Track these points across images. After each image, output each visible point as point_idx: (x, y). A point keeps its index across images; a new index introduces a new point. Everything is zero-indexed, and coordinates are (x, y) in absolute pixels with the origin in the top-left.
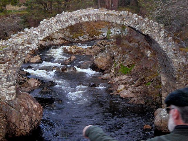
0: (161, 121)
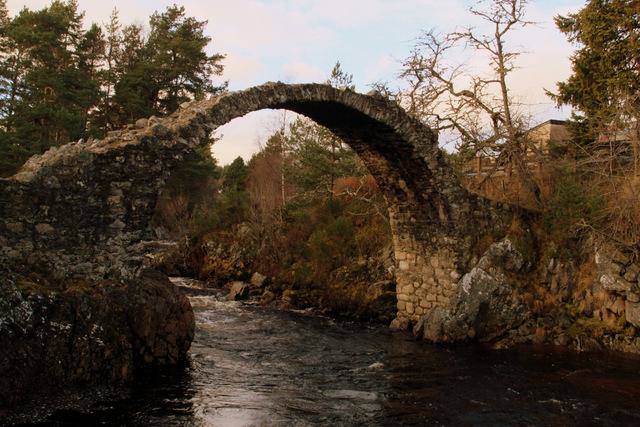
0: (442, 332)
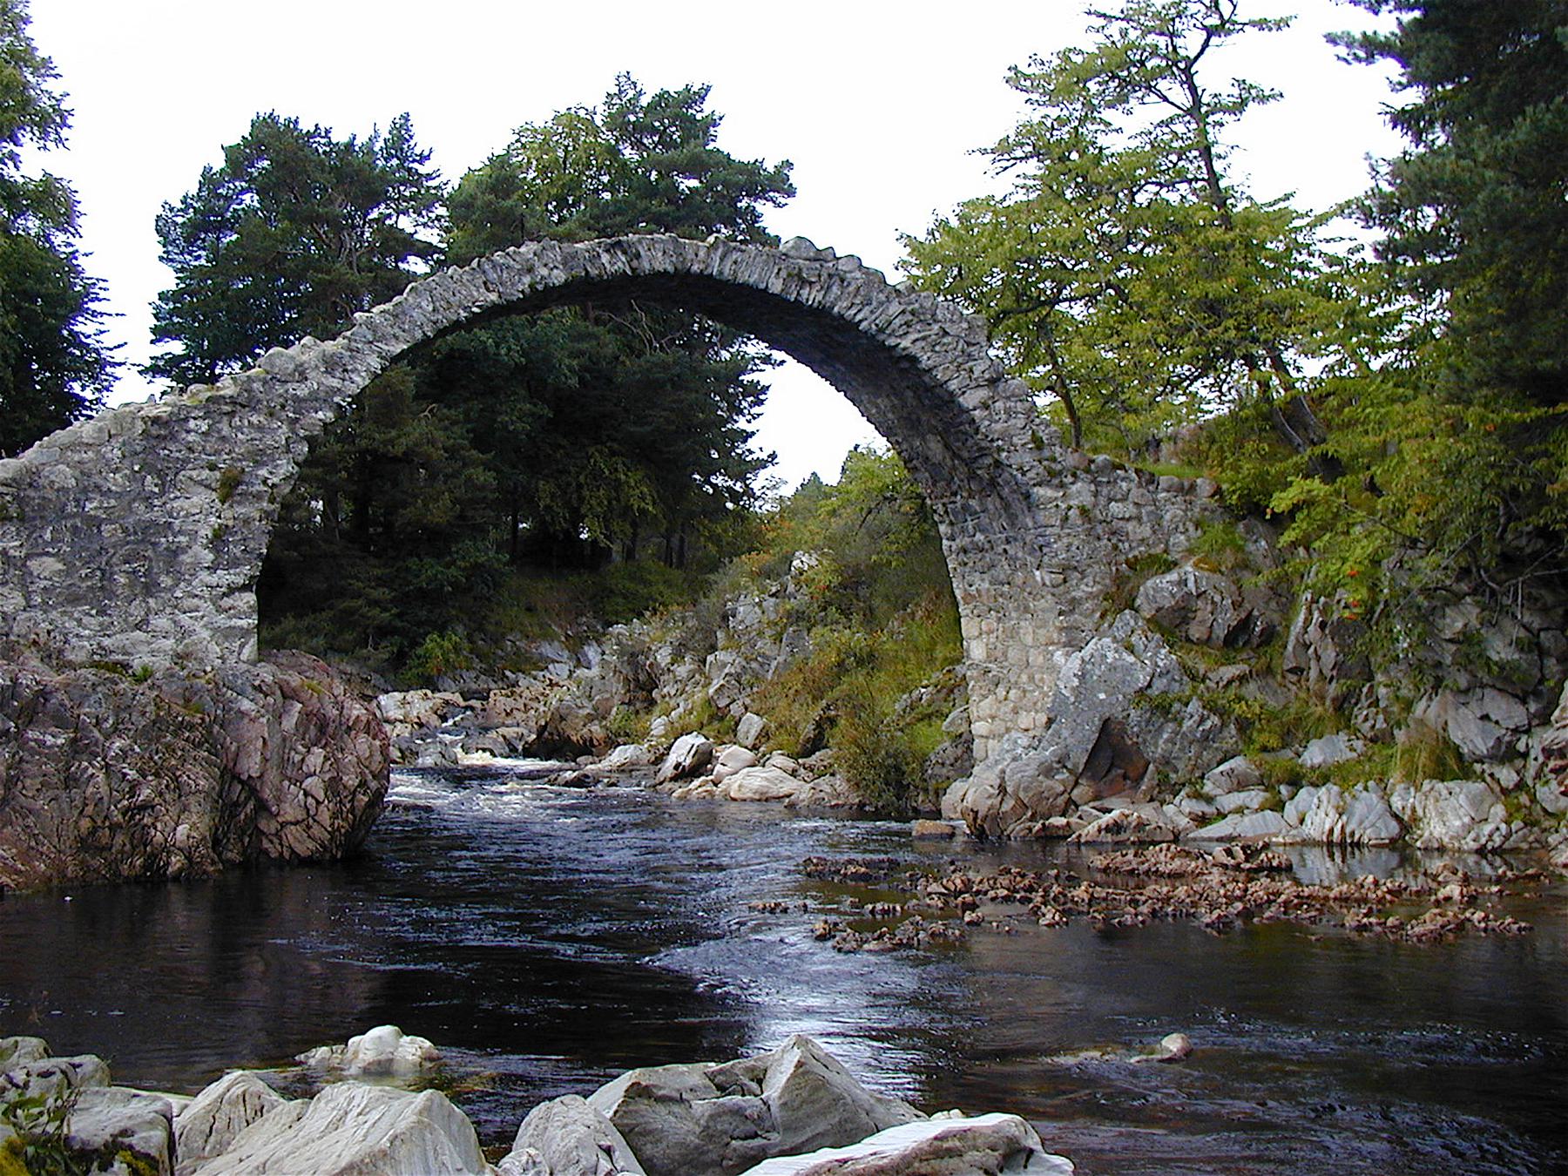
0: (1002, 789)
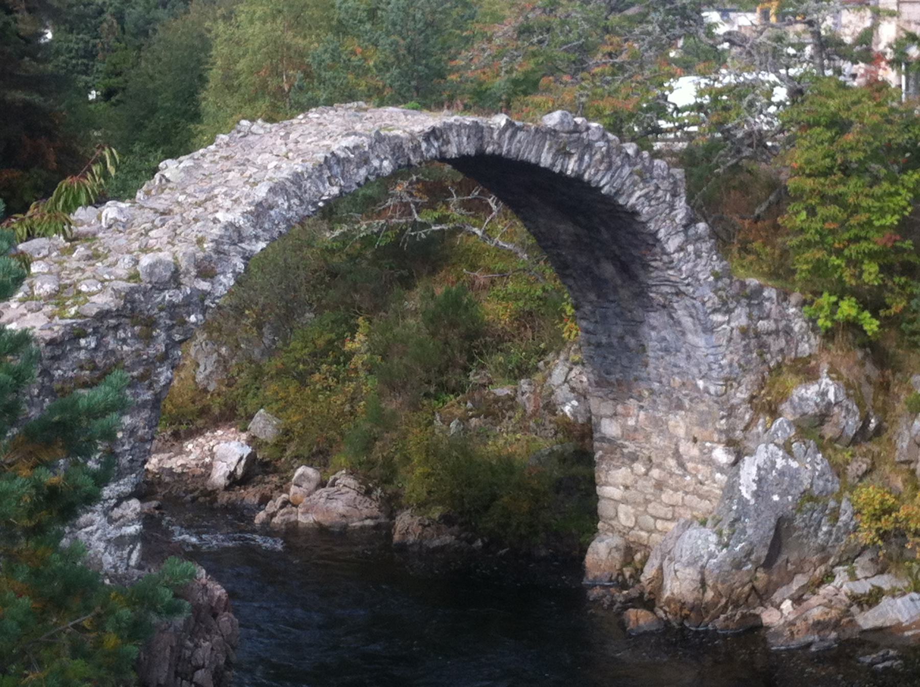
0: (703, 583)
